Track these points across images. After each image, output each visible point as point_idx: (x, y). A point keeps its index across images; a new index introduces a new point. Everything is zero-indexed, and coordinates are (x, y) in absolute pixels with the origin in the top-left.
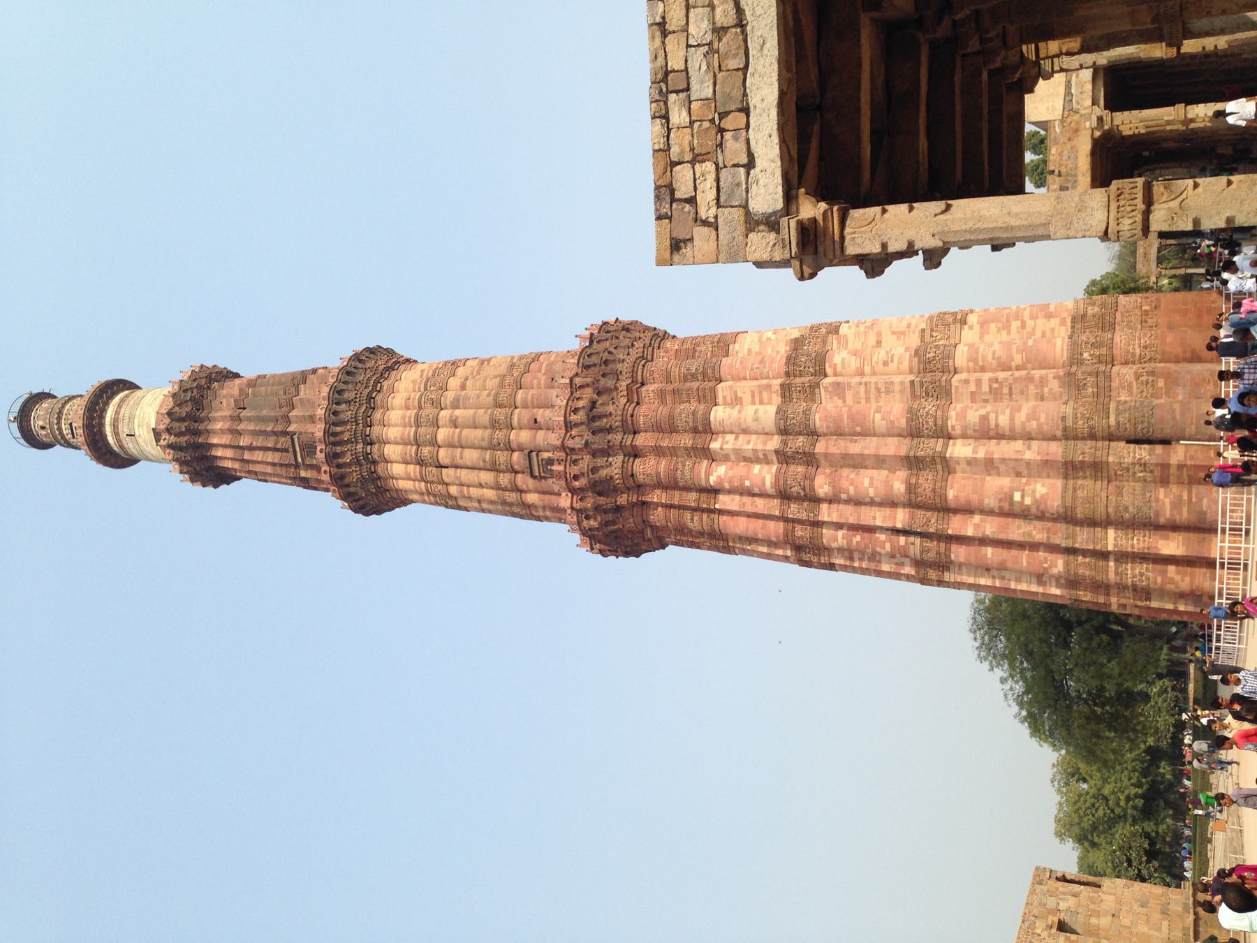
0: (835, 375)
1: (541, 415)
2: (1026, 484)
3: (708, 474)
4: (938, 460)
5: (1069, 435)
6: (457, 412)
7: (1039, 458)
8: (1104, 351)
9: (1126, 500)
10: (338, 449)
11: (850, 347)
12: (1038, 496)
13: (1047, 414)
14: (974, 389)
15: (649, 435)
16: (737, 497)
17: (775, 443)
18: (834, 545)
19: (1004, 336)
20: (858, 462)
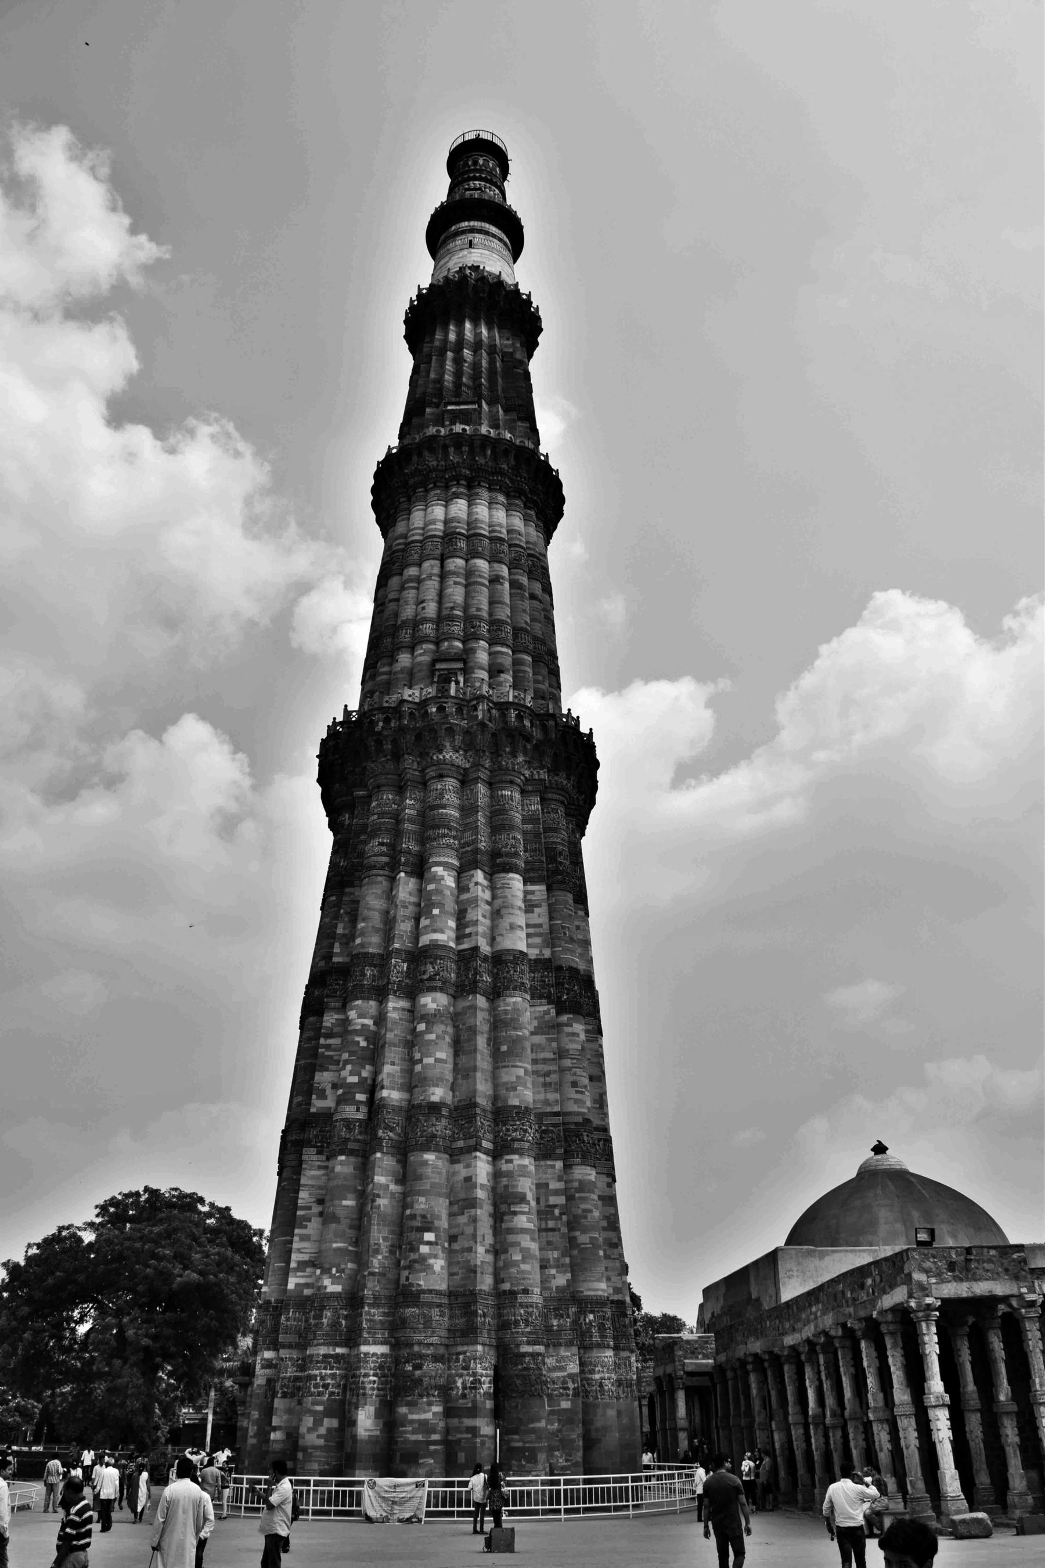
3: (446, 866)
4: (472, 1142)
5: (505, 1298)
6: (507, 585)
7: (479, 1263)
8: (596, 1338)
9: (429, 1367)
10: (465, 449)
12: (431, 1261)
13: (529, 1273)
14: (551, 1187)
16: (413, 899)
17: (485, 949)
18: (352, 1014)
20: (460, 1046)
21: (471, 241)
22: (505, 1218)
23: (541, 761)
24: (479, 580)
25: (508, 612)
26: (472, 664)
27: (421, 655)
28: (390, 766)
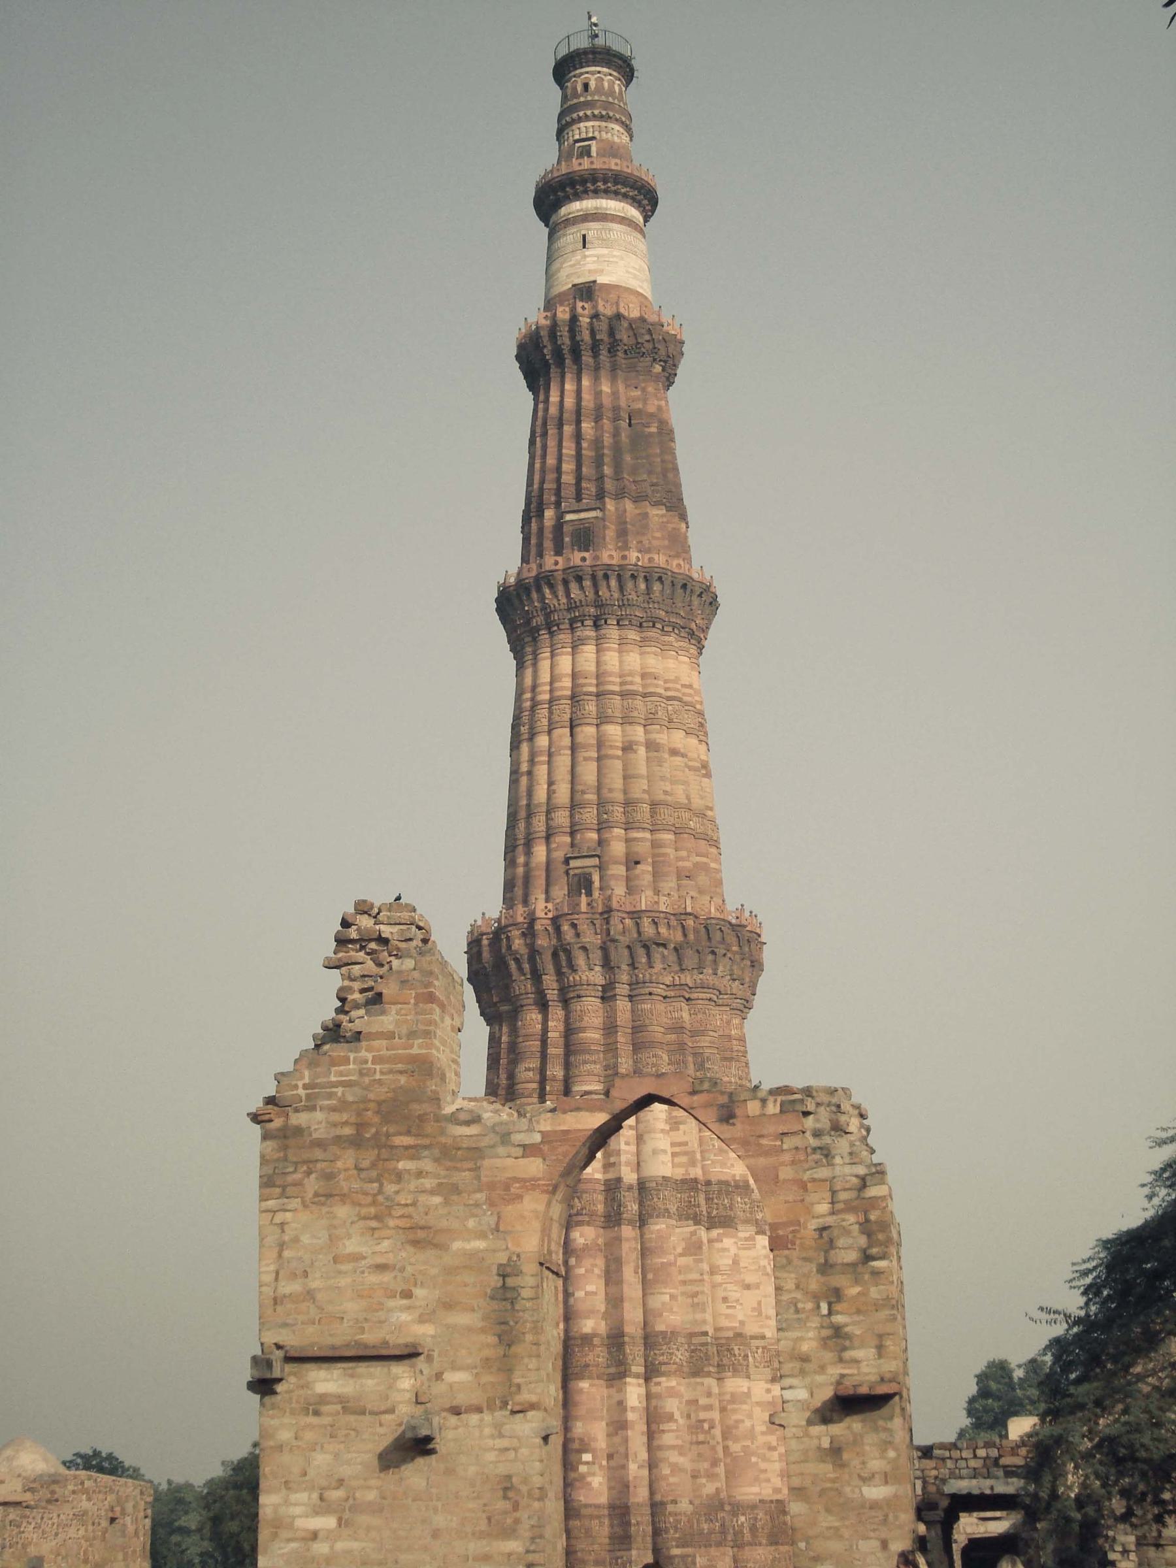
0: (710, 1241)
1: (645, 868)
2: (601, 1466)
4: (622, 1369)
5: (656, 1507)
6: (642, 751)
7: (631, 1478)
8: (747, 1536)
10: (587, 583)
11: (742, 1253)
12: (589, 1479)
14: (701, 1402)
15: (628, 1015)
17: (629, 1177)
19: (761, 1428)
20: (612, 1276)
21: (584, 236)
22: (656, 1435)
23: (680, 965)
24: (611, 752)
25: (644, 784)
26: (606, 858)
27: (556, 849)
28: (529, 987)
